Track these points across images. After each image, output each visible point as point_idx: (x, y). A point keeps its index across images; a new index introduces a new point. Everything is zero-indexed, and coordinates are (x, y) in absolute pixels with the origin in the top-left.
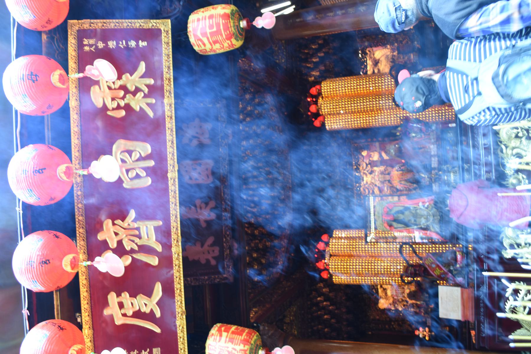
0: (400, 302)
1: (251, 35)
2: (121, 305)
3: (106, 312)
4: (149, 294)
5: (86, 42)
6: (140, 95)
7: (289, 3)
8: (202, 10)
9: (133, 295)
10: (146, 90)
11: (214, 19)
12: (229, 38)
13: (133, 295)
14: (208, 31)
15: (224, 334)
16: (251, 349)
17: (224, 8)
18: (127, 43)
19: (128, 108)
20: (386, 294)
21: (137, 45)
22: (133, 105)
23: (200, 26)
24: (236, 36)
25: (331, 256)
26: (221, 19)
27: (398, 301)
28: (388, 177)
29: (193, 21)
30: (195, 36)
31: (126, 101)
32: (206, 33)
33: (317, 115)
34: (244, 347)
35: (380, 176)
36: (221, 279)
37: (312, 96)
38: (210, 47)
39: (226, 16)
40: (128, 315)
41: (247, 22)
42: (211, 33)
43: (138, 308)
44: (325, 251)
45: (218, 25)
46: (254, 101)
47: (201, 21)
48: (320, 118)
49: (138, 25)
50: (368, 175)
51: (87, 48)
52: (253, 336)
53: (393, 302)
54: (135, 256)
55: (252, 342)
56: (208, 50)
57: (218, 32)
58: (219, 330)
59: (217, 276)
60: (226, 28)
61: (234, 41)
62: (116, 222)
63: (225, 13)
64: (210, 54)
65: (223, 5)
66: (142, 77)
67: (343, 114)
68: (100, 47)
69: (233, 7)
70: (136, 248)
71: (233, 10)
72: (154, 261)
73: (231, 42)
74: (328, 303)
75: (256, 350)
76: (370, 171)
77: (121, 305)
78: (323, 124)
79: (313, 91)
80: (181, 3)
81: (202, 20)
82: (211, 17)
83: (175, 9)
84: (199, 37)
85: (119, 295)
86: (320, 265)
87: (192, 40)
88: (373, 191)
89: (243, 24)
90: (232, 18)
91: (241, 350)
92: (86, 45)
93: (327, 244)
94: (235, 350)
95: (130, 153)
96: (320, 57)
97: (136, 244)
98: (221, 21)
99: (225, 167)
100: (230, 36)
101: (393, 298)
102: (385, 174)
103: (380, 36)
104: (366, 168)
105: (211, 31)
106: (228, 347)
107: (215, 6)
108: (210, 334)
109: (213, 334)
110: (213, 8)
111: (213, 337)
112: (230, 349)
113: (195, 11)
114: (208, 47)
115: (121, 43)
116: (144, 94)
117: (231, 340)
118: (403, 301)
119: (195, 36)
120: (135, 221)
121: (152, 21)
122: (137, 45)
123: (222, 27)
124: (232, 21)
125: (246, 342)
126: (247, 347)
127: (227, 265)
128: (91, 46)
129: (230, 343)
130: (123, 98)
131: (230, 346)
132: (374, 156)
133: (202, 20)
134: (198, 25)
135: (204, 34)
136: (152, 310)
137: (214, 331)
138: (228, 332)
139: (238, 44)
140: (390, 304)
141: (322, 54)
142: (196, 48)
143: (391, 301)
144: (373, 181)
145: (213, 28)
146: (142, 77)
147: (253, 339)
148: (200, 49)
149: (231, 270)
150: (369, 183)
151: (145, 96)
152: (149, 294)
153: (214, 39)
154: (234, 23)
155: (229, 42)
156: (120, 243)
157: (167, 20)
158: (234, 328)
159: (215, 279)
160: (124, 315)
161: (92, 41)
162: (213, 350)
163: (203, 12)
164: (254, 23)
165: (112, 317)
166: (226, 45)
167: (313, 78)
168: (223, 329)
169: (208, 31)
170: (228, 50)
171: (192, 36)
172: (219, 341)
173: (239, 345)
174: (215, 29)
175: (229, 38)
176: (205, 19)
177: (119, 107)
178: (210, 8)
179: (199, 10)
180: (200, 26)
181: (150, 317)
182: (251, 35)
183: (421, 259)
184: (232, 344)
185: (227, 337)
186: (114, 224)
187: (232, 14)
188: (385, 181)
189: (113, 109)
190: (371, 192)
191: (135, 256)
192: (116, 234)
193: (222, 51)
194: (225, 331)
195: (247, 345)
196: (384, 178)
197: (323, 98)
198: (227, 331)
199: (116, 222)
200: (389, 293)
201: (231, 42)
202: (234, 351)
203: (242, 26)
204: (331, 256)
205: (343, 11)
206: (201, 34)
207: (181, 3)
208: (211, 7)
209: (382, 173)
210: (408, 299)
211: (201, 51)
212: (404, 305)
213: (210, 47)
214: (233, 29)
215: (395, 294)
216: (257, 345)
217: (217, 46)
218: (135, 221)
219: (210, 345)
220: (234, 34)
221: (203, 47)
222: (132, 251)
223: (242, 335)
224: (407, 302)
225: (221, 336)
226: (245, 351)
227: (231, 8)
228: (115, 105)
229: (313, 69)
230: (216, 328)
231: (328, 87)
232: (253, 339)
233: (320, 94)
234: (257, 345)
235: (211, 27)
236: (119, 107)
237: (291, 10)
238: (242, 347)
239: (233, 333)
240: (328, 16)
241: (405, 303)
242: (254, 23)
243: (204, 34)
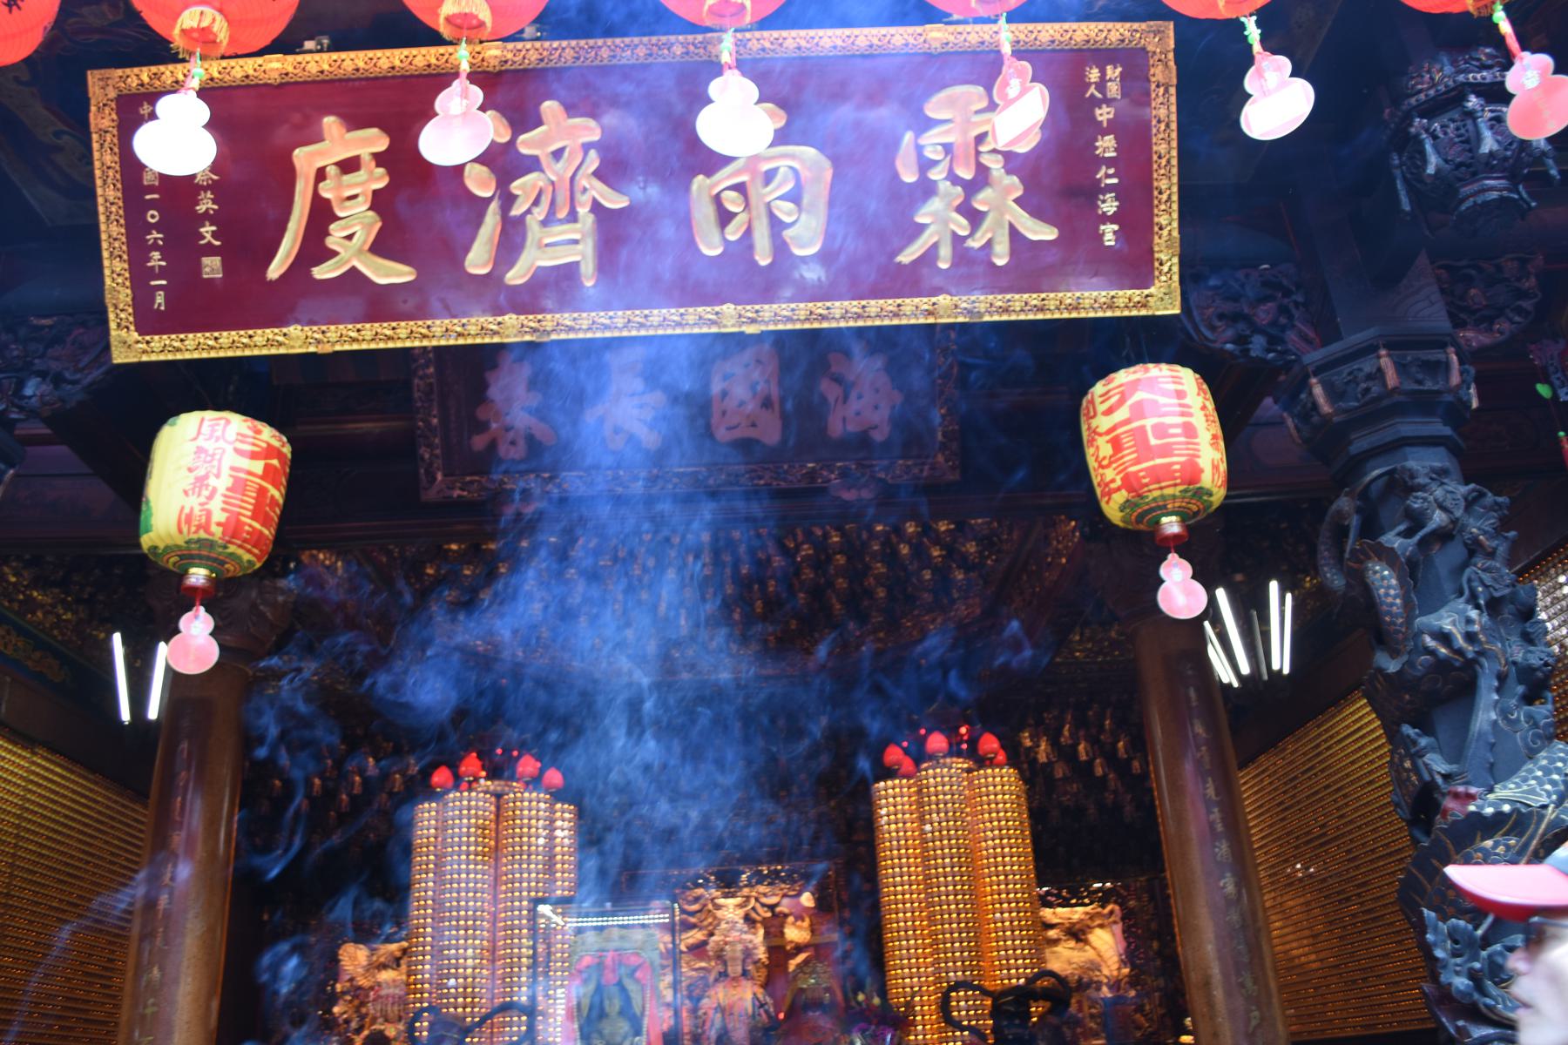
0: (357, 1009)
1: (1141, 549)
2: (349, 166)
3: (330, 122)
4: (380, 247)
5: (1113, 72)
6: (961, 225)
7: (1245, 669)
8: (1210, 405)
9: (379, 201)
10: (975, 244)
11: (1182, 439)
12: (1129, 483)
13: (379, 201)
14: (1149, 423)
15: (258, 466)
16: (211, 544)
17: (1215, 467)
18: (1110, 188)
19: (926, 189)
20: (384, 966)
21: (1105, 219)
22: (935, 204)
23: (1162, 400)
24: (1135, 505)
25: (498, 796)
26: (1182, 459)
27: (363, 1004)
29: (1177, 380)
30: (1134, 386)
31: (944, 186)
32: (1142, 417)
33: (920, 756)
34: (219, 524)
35: (740, 947)
36: (431, 464)
37: (973, 742)
38: (1102, 430)
39: (1191, 474)
40: (321, 185)
41: (1176, 537)
42: (1142, 429)
43: (340, 214)
44: (512, 778)
45: (1166, 451)
46: (959, 567)
47: (1176, 401)
48: (907, 764)
49: (1163, 220)
50: (741, 912)
51: (1094, 75)
52: (249, 551)
53: (360, 988)
54: (494, 207)
55: (232, 549)
56: (1094, 423)
57: (1145, 451)
58: (270, 452)
59: (438, 452)
60: (1158, 475)
61: (1120, 497)
62: (593, 154)
63: (1201, 471)
64: (1084, 427)
65: (1223, 467)
66: (1014, 233)
67: (923, 832)
68: (1098, 112)
69: (1219, 495)
70: (516, 211)
71: (1210, 494)
72: (478, 260)
73: (1119, 489)
74: (357, 790)
75: (208, 558)
76: (753, 915)
77: (349, 166)
78: (888, 773)
79: (990, 743)
80: (1229, 346)
81: (1181, 405)
82: (1189, 431)
83: (1213, 328)
84: (1131, 395)
85: (379, 159)
86: (470, 765)
87: (1122, 377)
88: (693, 926)
89: (1171, 525)
90: (1185, 491)
91: (209, 514)
92: (1103, 73)
93: (535, 782)
94: (210, 497)
95: (795, 197)
96: (1090, 763)
97: (529, 211)
98: (1177, 460)
99: (760, 478)
100: (1135, 484)
101: (372, 988)
102: (744, 961)
103: (1155, 945)
104: (763, 905)
105: (1149, 429)
106: (218, 476)
107: (1222, 444)
108: (259, 425)
109: (258, 432)
110: (1214, 437)
111: (250, 433)
112: (212, 481)
113: (1205, 386)
114: (1103, 423)
115: (1111, 171)
116: (965, 238)
117: (238, 486)
118: (362, 1017)
119: (1134, 386)
120: (596, 207)
121: (1176, 260)
122: (1105, 219)
123: (1159, 461)
124: (1177, 491)
125: (233, 529)
126: (217, 531)
127: (472, 482)
128: (1102, 85)
129: (229, 482)
130: (954, 179)
131: (223, 483)
132: (800, 928)
133: (1181, 405)
134: (1165, 393)
135: (1139, 411)
136: (334, 254)
137: (268, 435)
138: (262, 477)
139: (1113, 508)
140: (351, 980)
141: (1099, 771)
142: (1099, 388)
143: (362, 982)
144: (723, 926)
145: (1157, 437)
146: (1014, 233)
147: (240, 552)
148: (1098, 400)
149: (457, 493)
150: (719, 913)
151: (957, 240)
152: (380, 247)
153: (1127, 441)
154: (1174, 497)
155: (1119, 483)
156: (533, 164)
157: (1178, 303)
158: (277, 494)
159: (430, 446)
160: (321, 175)
161: (1113, 89)
162: (213, 431)
163: (1204, 408)
164: (1173, 558)
165: (318, 138)
166: (1109, 474)
167: (1028, 743)
168: (275, 462)
169: (1149, 423)
170: (1096, 481)
171: (1133, 377)
172: (239, 452)
173: (224, 510)
174: (1153, 442)
175: (1129, 483)
176: (1183, 414)
177: (925, 165)
178: (1216, 429)
179: (1209, 395)
180: (1162, 400)
181: (315, 248)
182: (1141, 549)
184: (228, 489)
185: (250, 473)
186: (586, 147)
187: (1200, 493)
188: (725, 963)
189: (919, 149)
190: (693, 920)
191: (494, 207)
192: (557, 154)
193: (1092, 463)
194: (267, 467)
195: (224, 533)
196: (734, 959)
197: (969, 771)
198: (268, 473)
199: (593, 154)
200: (386, 976)
201: (1119, 489)
202: (206, 493)
203: (1164, 520)
204: (498, 796)
205: (1219, 827)
206: (1139, 404)
207: (1229, 346)
208: (1220, 433)
209: (748, 953)
210: (366, 1032)
211: (1092, 402)
212: (347, 1022)
213: (1102, 430)
214: (1157, 493)
215: (383, 992)
216: (223, 563)
217: (1106, 450)
218: (596, 207)
219: (228, 422)
220: (1140, 496)
221: (1101, 408)
222: (508, 200)
223: (253, 518)
224: (358, 1031)
225: (254, 456)
226: (206, 527)
227: (1215, 490)
228: (931, 154)
229: (1054, 743)
230: (276, 444)
231: (1002, 783)
232: (240, 552)
233: (982, 762)
234: (223, 563)
235: (1161, 431)
236: (925, 165)
237: (1225, 674)
238: (219, 516)
239: (262, 491)
240: (1205, 782)
241: (354, 1025)
242: (1173, 558)
243: (1139, 411)
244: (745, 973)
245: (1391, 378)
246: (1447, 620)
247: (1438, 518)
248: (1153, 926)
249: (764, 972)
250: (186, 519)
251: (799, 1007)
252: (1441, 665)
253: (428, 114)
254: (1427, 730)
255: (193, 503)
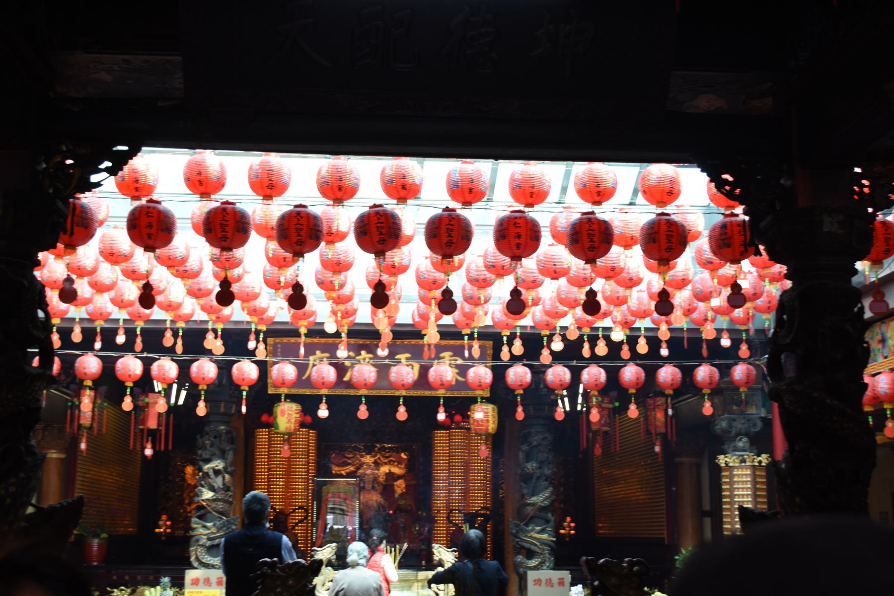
3: (318, 352)
7: (568, 409)
15: (298, 415)
28: (368, 486)
39: (487, 429)
50: (373, 459)
82: (488, 421)
88: (349, 464)
103: (562, 489)
131: (293, 421)
132: (400, 468)
150: (363, 460)
183: (294, 527)
188: (364, 483)
209: (375, 479)
244: (373, 488)
245: (532, 412)
246: (529, 466)
247: (535, 443)
248: (562, 480)
249: (381, 487)
250: (287, 428)
251: (399, 509)
252: (528, 474)
253: (338, 349)
254: (525, 483)
255: (288, 425)
